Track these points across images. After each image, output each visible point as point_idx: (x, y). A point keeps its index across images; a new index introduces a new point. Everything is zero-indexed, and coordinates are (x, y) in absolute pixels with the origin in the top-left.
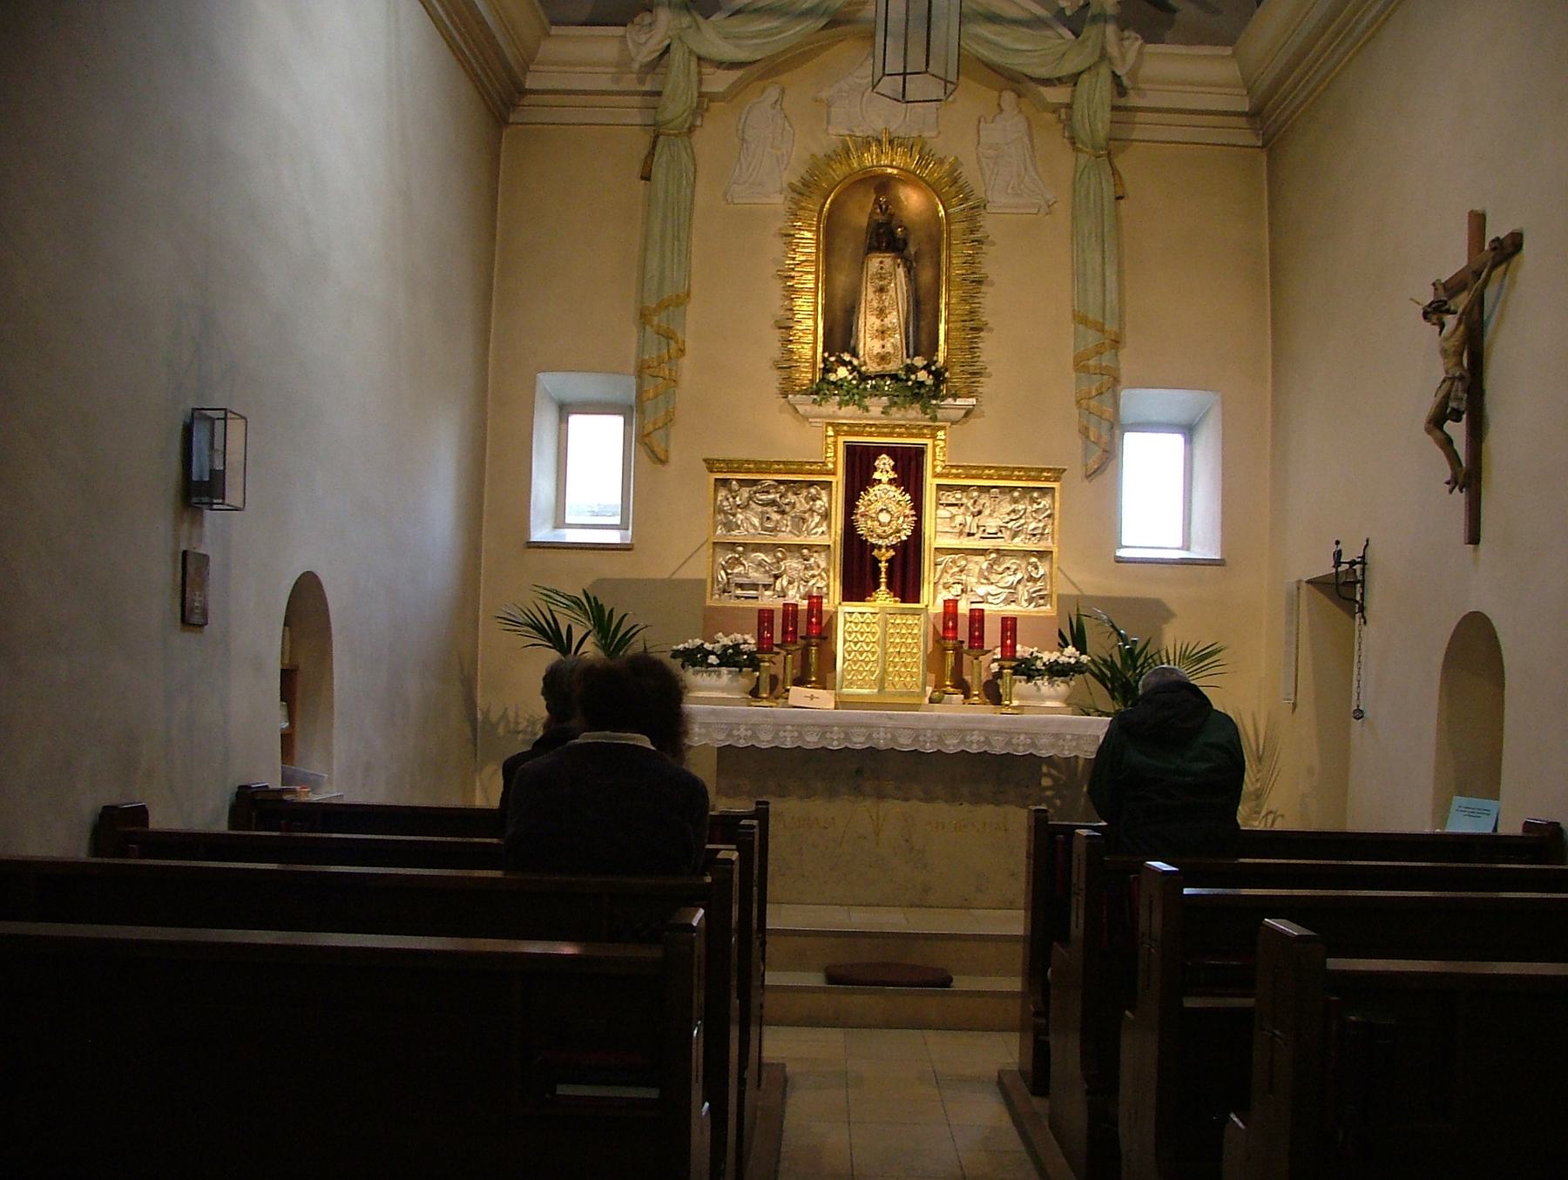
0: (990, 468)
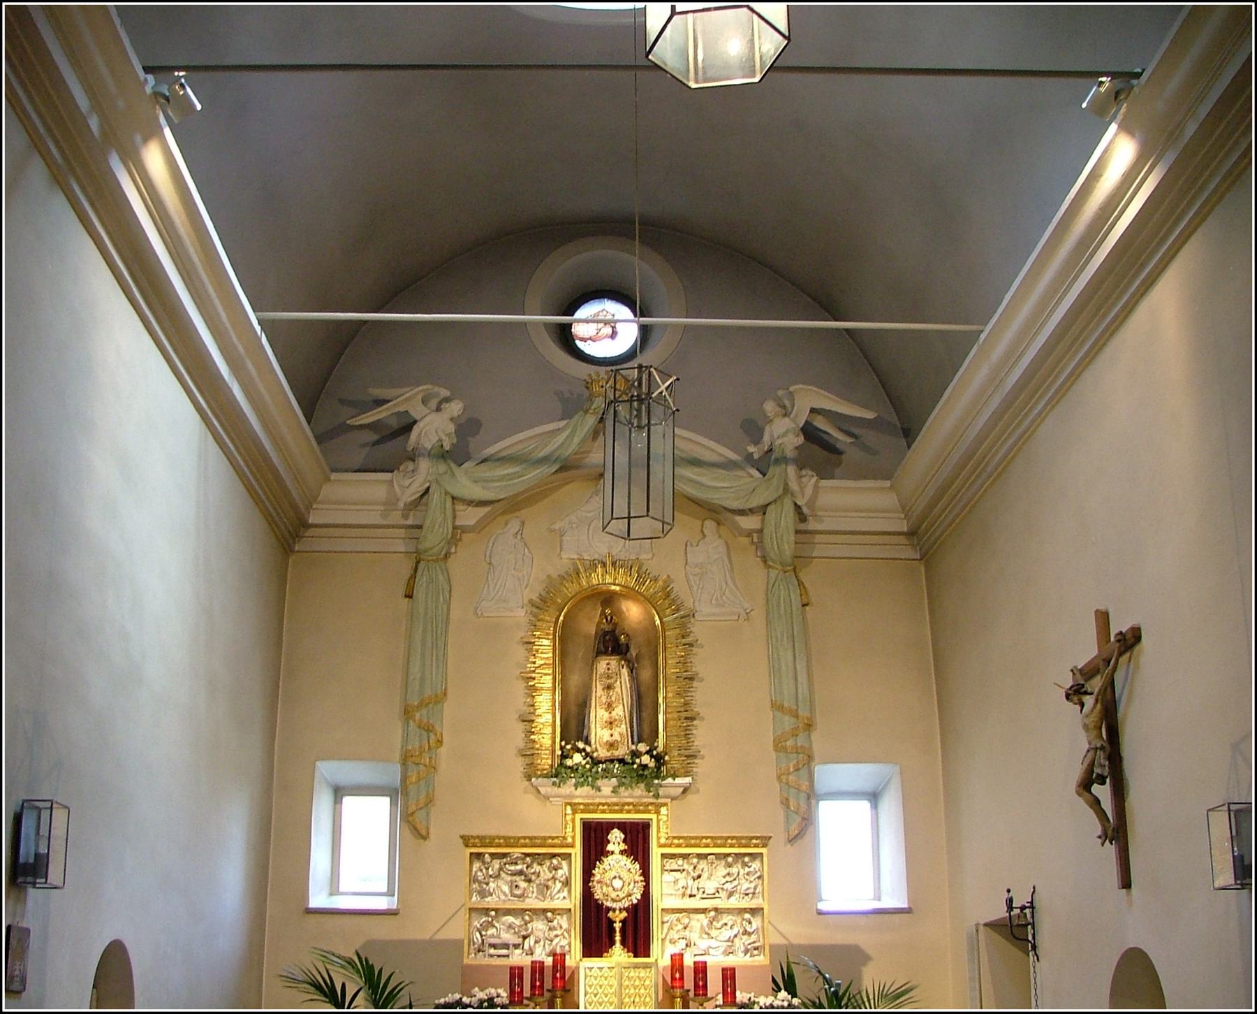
0: (707, 838)
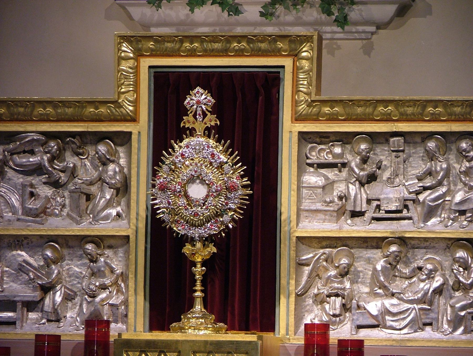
0: (386, 103)
